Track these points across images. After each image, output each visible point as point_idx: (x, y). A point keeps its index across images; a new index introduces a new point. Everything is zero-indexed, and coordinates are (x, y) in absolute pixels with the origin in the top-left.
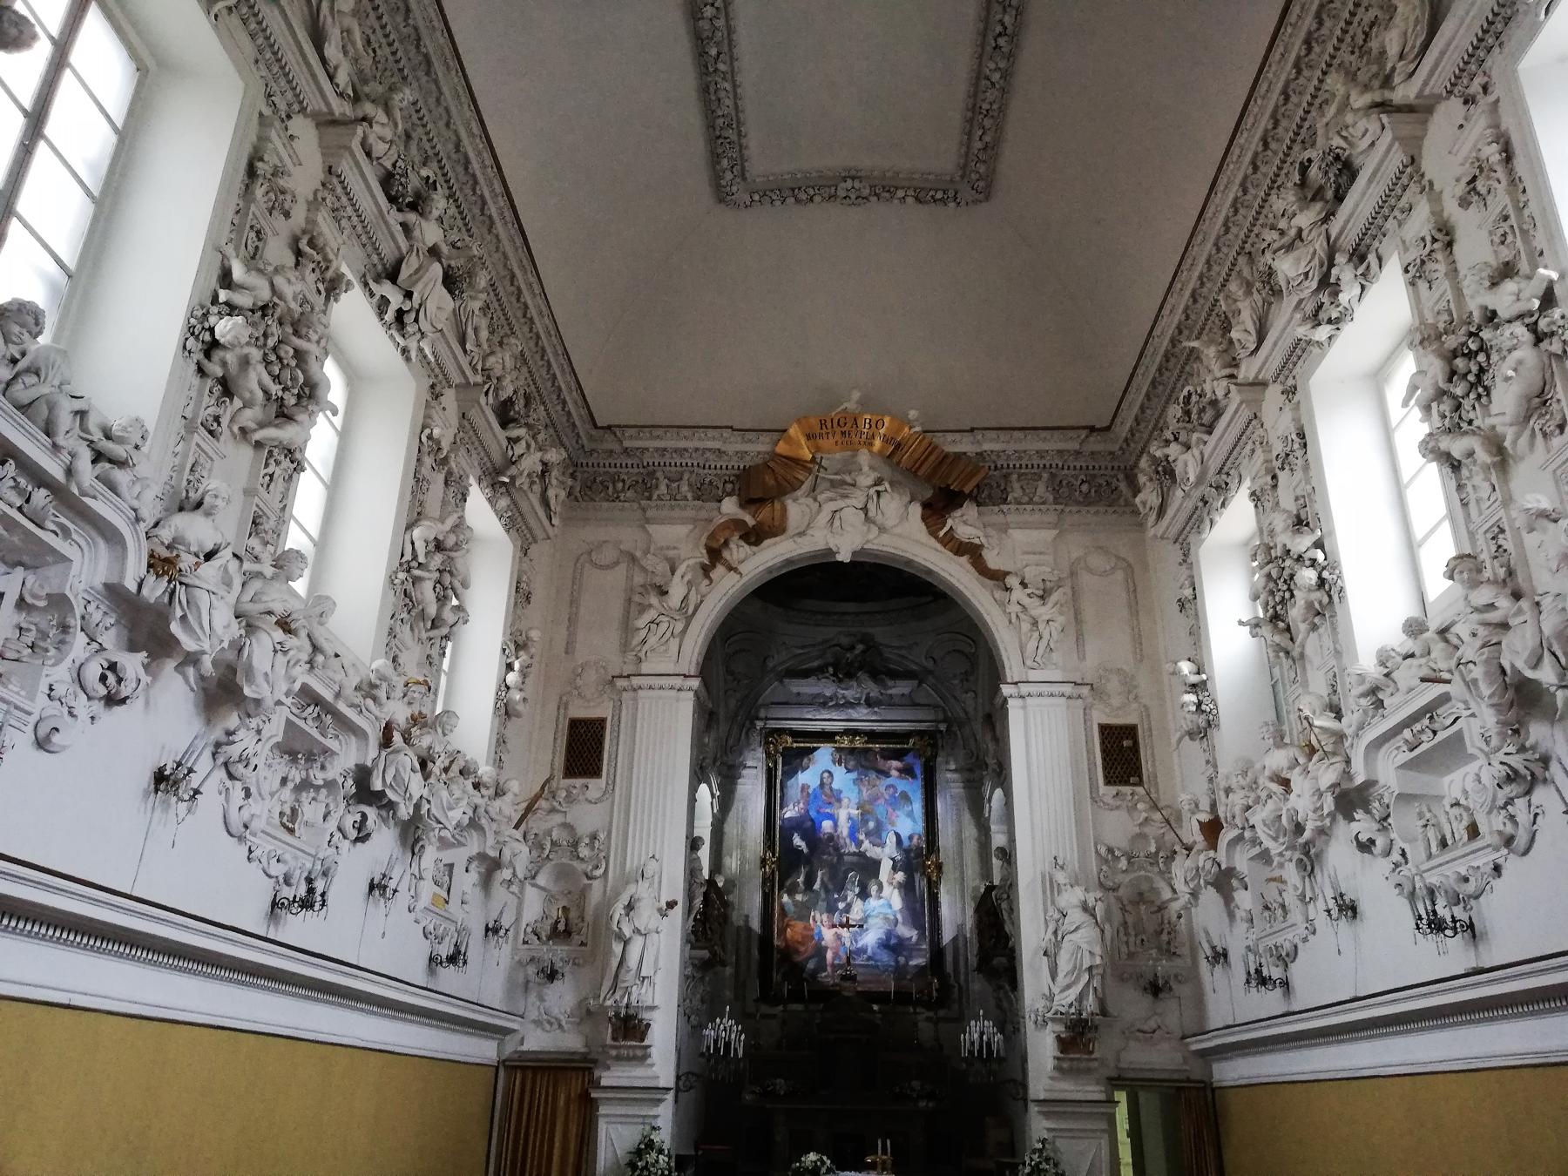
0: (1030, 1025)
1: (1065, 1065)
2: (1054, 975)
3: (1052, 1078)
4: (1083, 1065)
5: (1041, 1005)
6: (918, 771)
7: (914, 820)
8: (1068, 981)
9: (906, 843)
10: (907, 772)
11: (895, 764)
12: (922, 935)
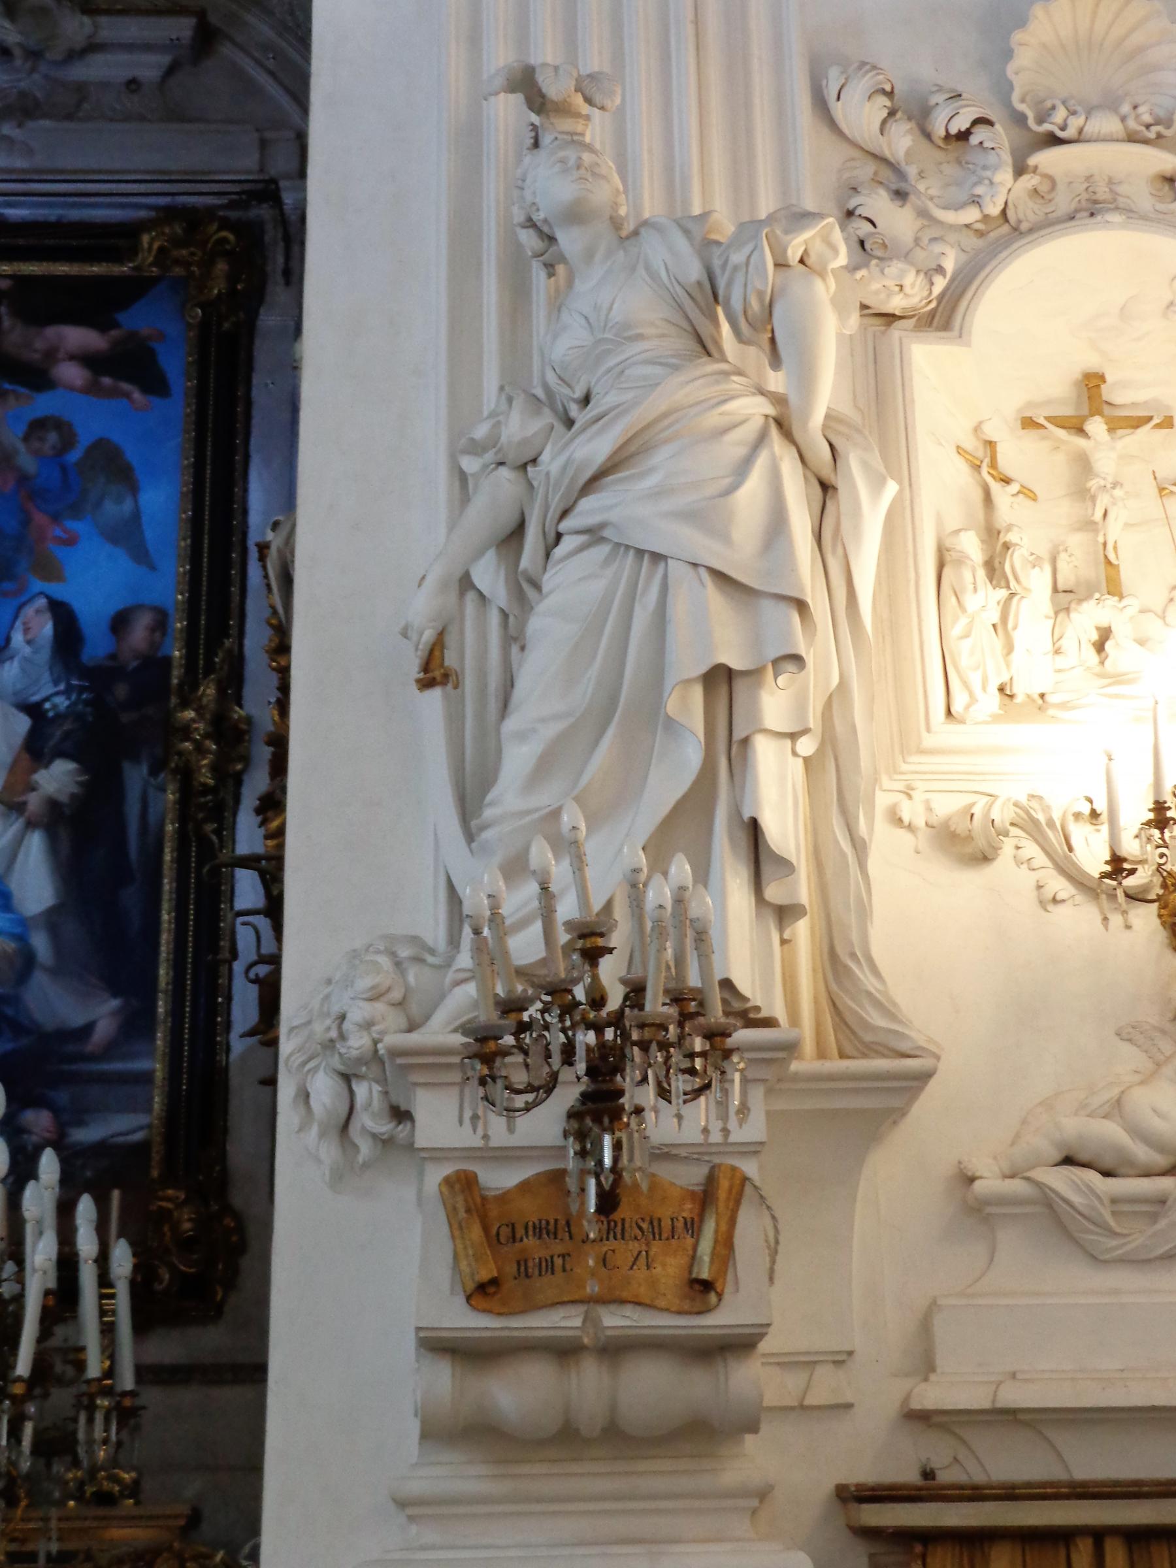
2: (470, 800)
6: (176, 362)
7: (141, 555)
9: (97, 646)
10: (130, 366)
11: (77, 337)
12: (136, 1025)
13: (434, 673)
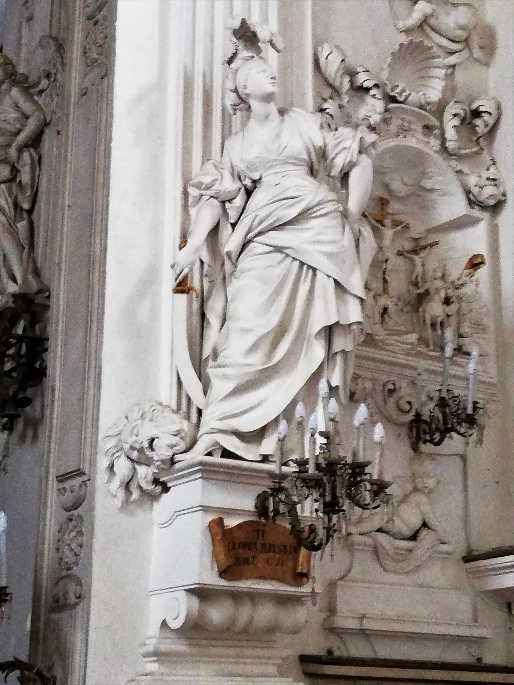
0: (106, 496)
1: (217, 614)
3: (158, 655)
4: (265, 613)
5: (166, 431)
8: (257, 361)
13: (182, 287)
